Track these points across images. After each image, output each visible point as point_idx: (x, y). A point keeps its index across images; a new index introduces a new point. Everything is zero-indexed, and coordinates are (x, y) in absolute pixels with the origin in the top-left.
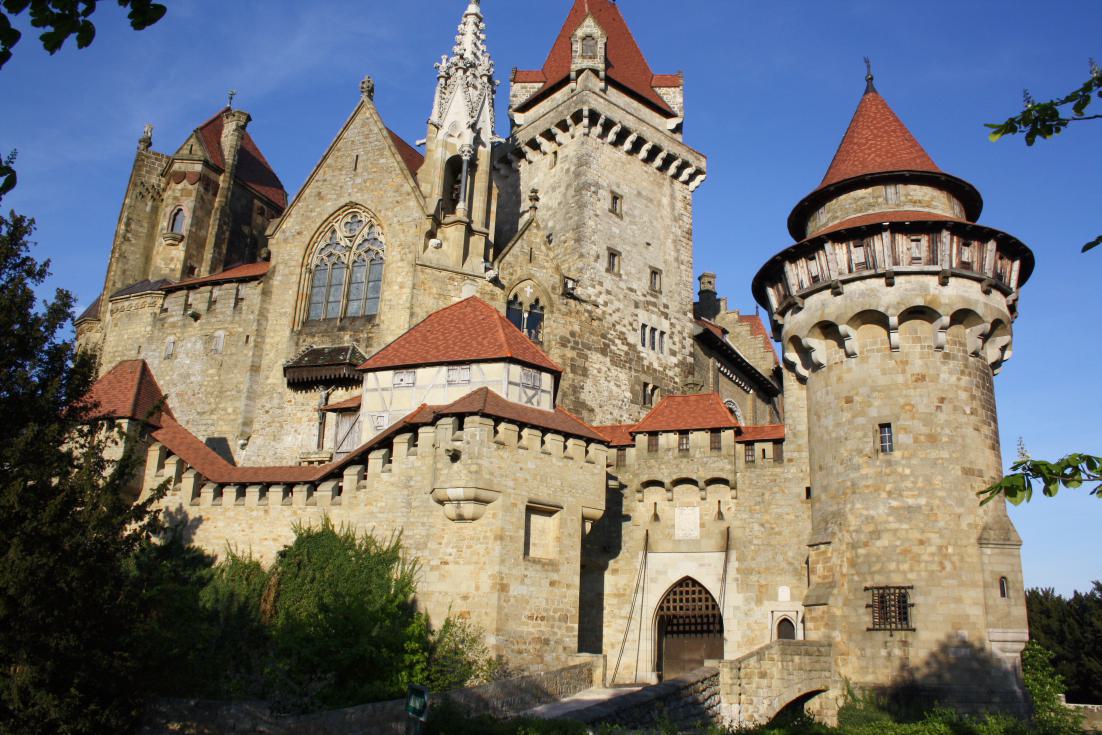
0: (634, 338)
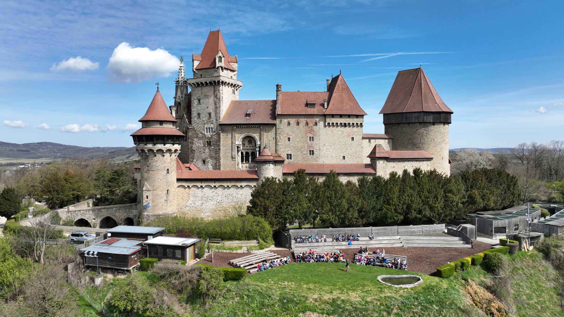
0: (203, 132)
